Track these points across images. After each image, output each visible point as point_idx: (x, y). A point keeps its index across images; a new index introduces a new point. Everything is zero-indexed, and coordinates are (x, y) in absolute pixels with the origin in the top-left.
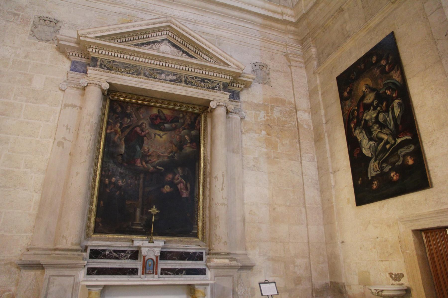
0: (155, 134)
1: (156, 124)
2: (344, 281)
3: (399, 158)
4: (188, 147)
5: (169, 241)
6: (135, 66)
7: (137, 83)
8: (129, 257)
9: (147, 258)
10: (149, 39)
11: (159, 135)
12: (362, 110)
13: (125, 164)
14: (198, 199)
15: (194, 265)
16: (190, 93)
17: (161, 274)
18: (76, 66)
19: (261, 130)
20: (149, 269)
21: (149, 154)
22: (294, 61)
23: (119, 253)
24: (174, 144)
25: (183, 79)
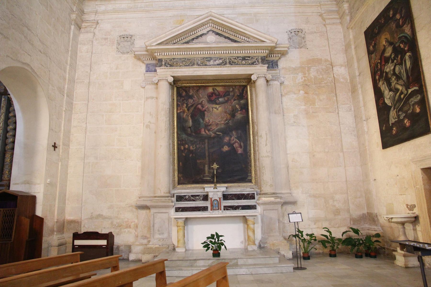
0: (212, 108)
1: (213, 100)
2: (376, 211)
3: (410, 107)
4: (239, 114)
5: (230, 186)
6: (189, 58)
7: (193, 72)
8: (202, 199)
9: (213, 199)
10: (197, 34)
11: (216, 108)
12: (383, 63)
13: (194, 134)
14: (250, 153)
15: (247, 203)
16: (235, 72)
17: (224, 210)
18: (149, 67)
19: (299, 91)
20: (216, 207)
21: (210, 124)
22: (329, 19)
23: (195, 197)
24: (228, 114)
25: (228, 61)
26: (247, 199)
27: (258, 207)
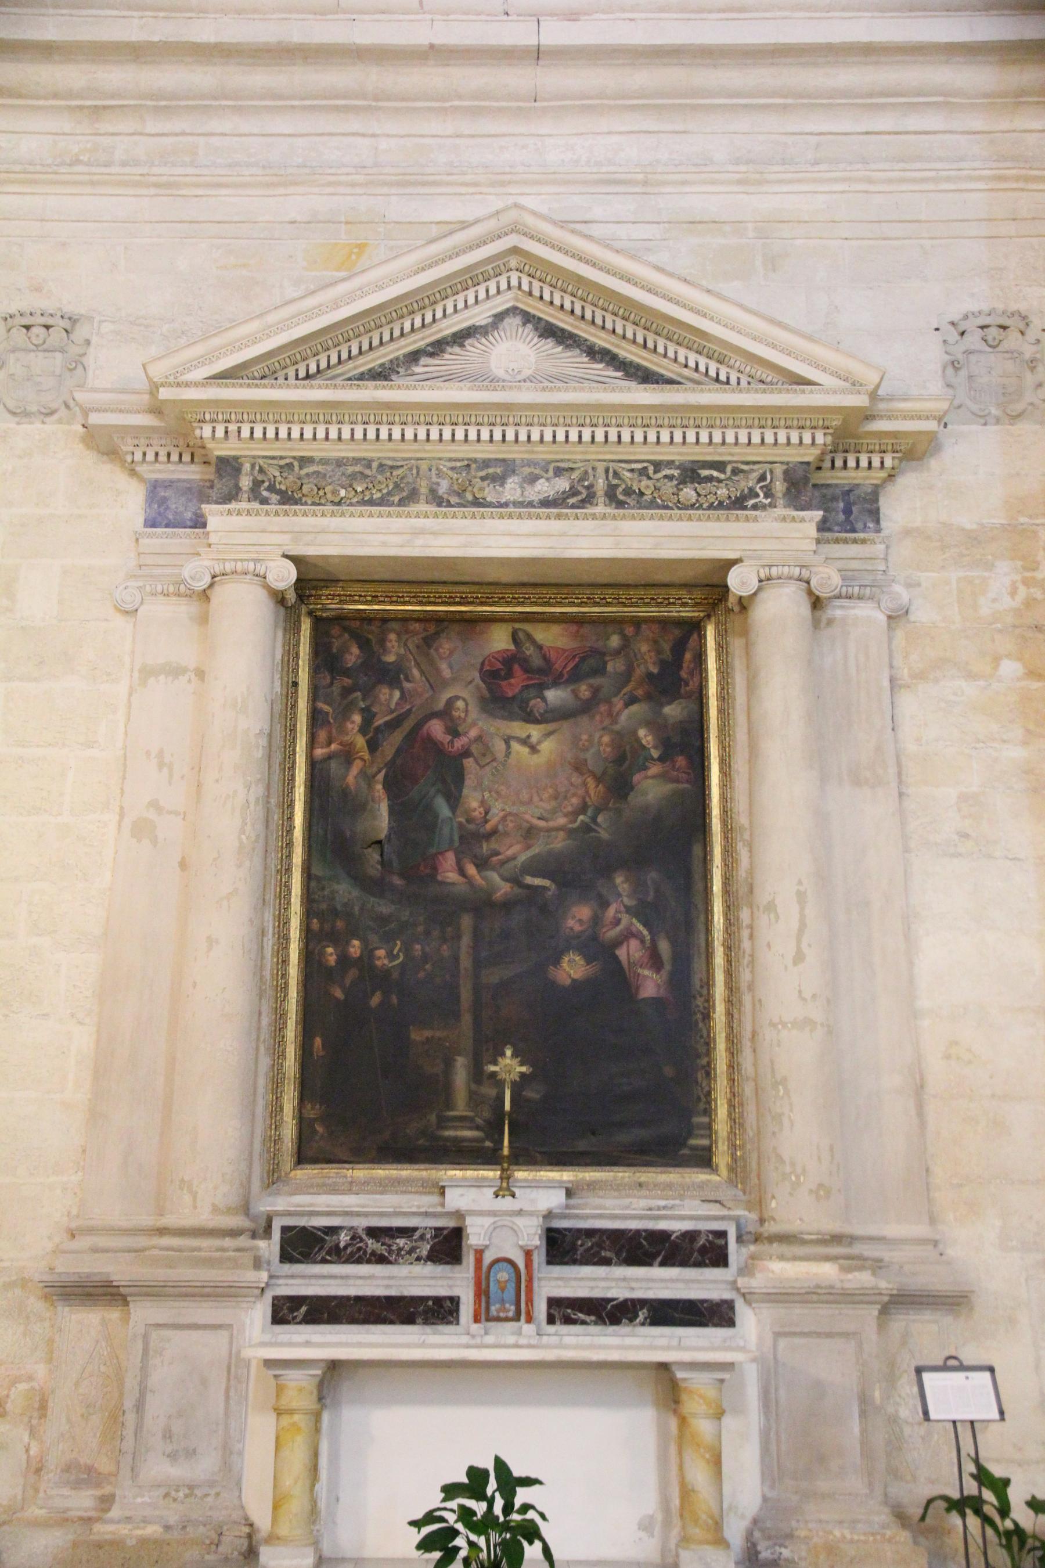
0: (507, 741)
1: (510, 694)
4: (653, 777)
5: (592, 1186)
6: (390, 463)
7: (407, 537)
8: (425, 1253)
9: (488, 1258)
10: (435, 328)
11: (525, 741)
13: (397, 881)
14: (708, 1001)
15: (680, 1285)
17: (551, 1320)
18: (163, 501)
19: (997, 660)
20: (503, 1302)
21: (488, 827)
23: (387, 1240)
24: (593, 774)
25: (601, 484)
26: (684, 1264)
27: (744, 1314)
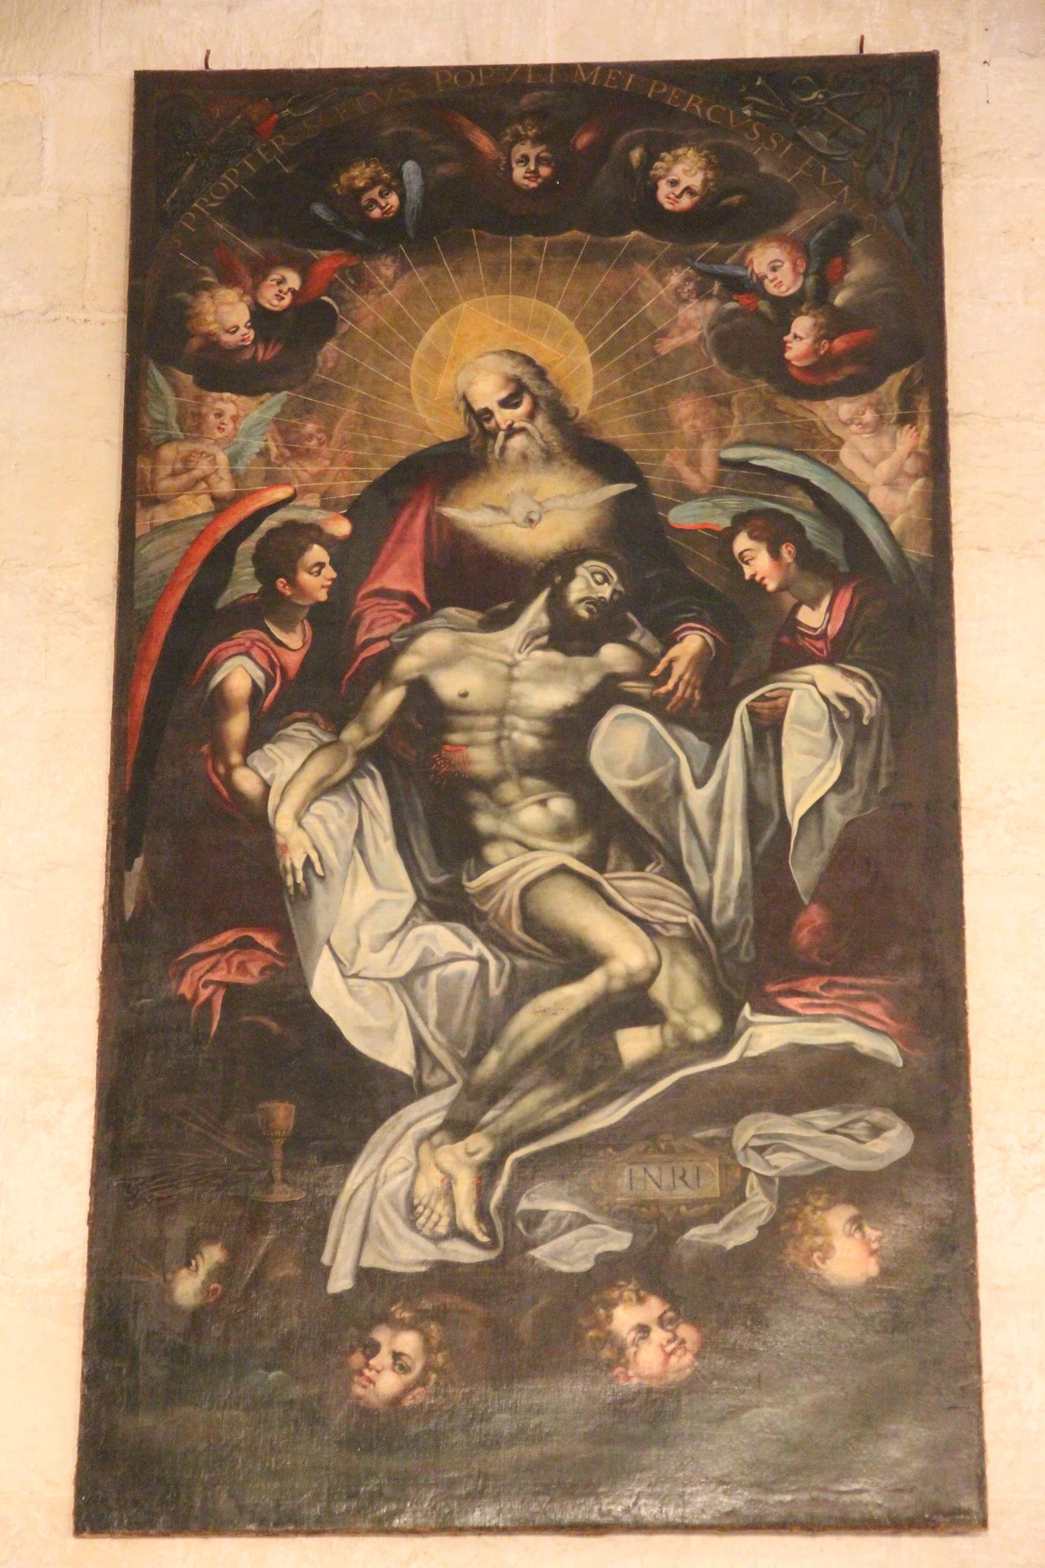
3: (738, 1196)
